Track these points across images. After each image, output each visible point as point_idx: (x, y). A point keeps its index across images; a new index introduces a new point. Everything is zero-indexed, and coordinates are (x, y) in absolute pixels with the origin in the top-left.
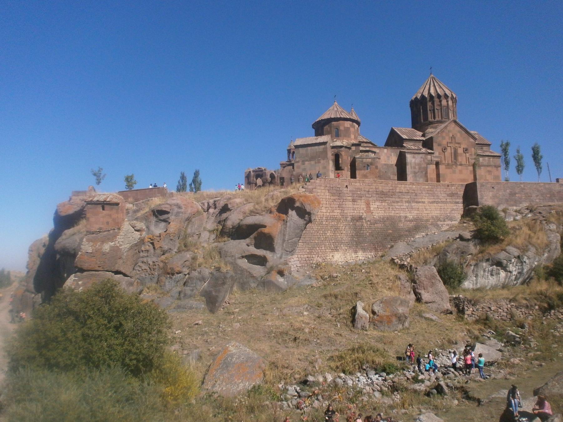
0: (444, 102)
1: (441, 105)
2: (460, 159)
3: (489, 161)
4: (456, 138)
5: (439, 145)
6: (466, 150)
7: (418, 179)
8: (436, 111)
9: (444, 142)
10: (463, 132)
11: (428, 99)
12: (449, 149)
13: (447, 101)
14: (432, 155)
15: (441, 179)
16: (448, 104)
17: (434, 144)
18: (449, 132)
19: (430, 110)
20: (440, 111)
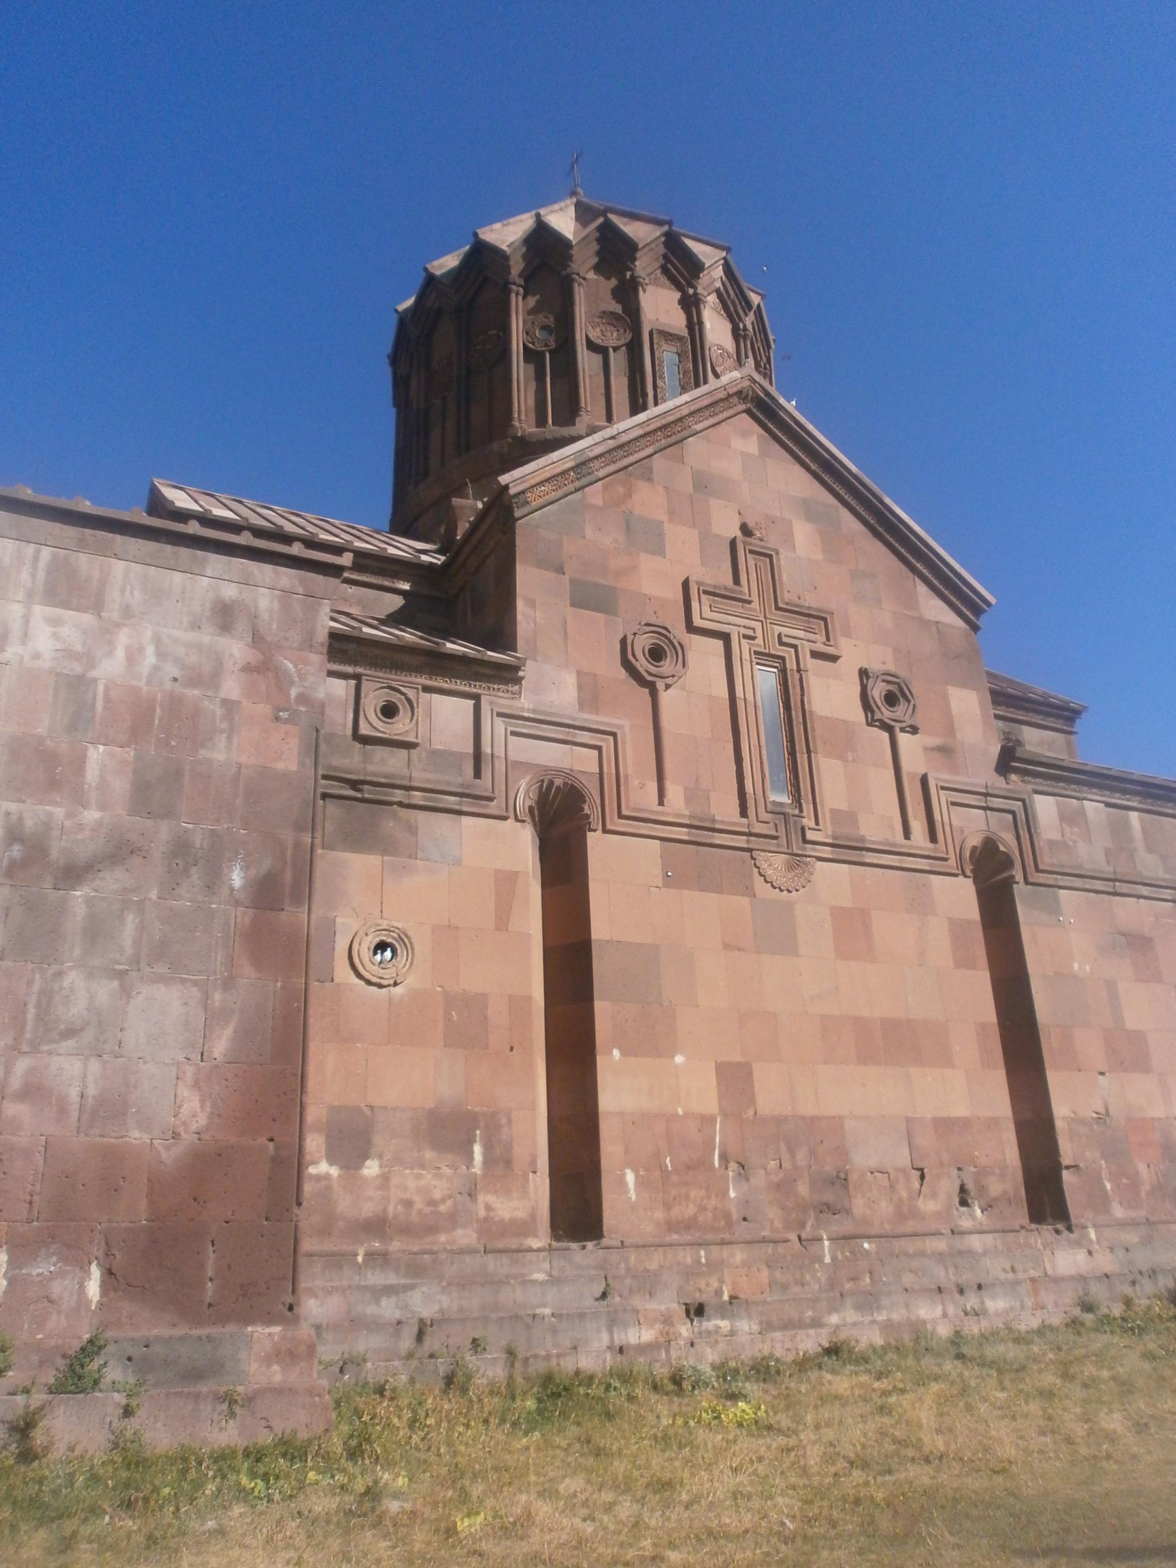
0: (660, 306)
1: (628, 312)
2: (832, 779)
3: (1120, 832)
4: (784, 561)
5: (592, 597)
6: (888, 701)
7: (81, 991)
8: (587, 362)
9: (655, 582)
10: (849, 522)
11: (516, 267)
12: (704, 656)
13: (691, 305)
14: (495, 698)
15: (602, 1009)
16: (695, 326)
17: (528, 579)
18: (703, 484)
19: (531, 355)
20: (618, 362)
